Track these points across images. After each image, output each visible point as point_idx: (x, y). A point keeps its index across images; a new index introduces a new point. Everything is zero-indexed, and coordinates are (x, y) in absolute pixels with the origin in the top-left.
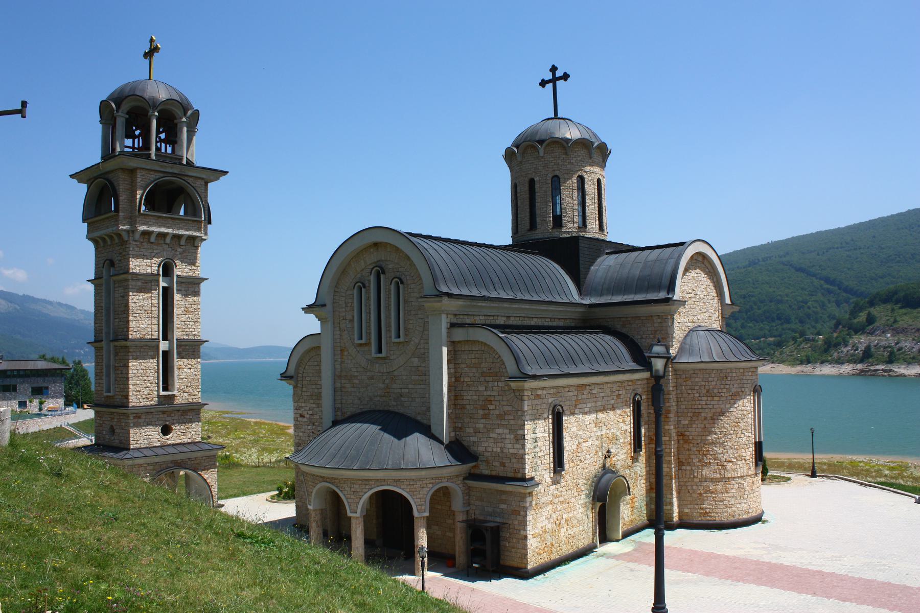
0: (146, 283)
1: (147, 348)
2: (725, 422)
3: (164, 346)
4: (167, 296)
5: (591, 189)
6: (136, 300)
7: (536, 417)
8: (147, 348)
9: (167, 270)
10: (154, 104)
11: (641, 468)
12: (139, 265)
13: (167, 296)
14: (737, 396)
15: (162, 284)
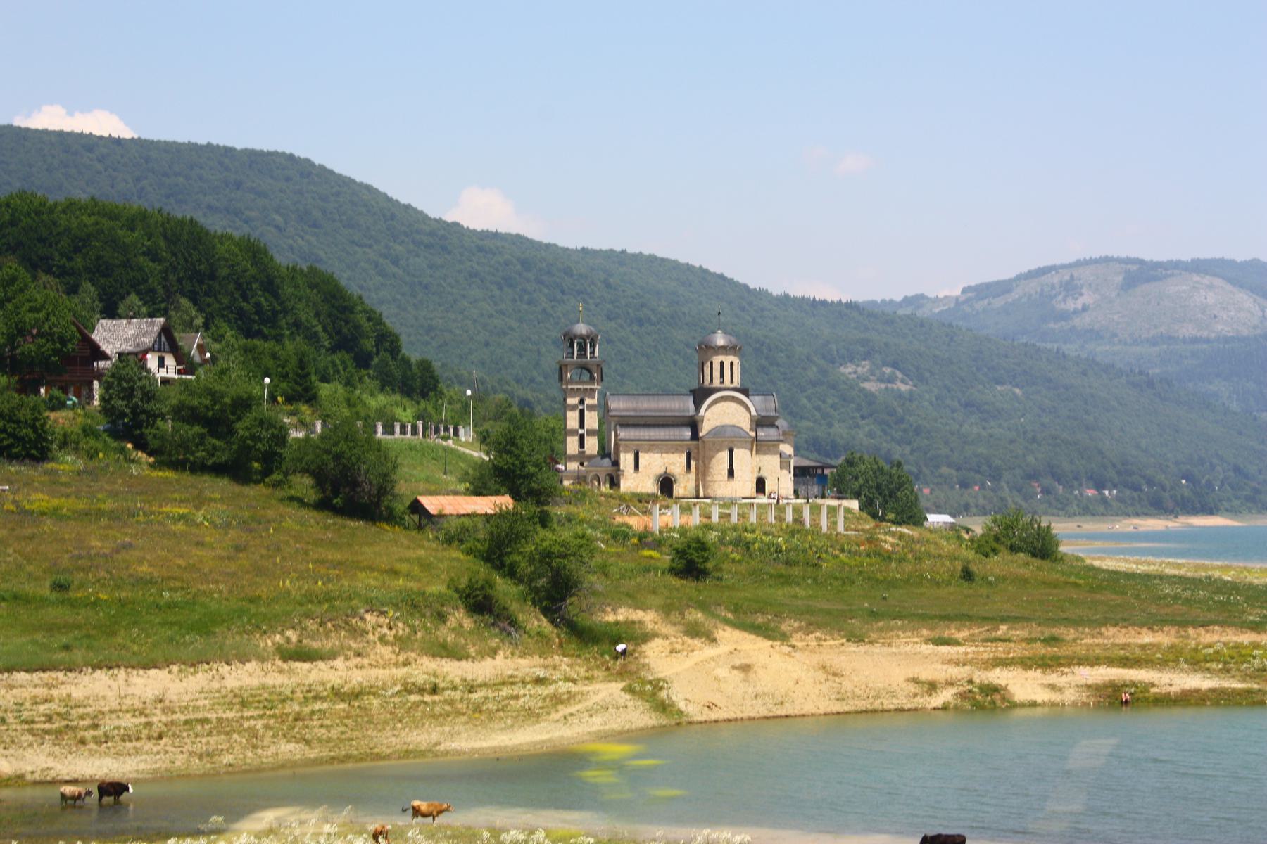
0: (574, 408)
1: (574, 432)
2: (714, 461)
3: (581, 431)
4: (582, 412)
5: (717, 367)
6: (569, 414)
7: (626, 452)
8: (574, 432)
9: (582, 402)
10: (576, 337)
11: (692, 475)
12: (570, 401)
13: (582, 412)
14: (719, 451)
15: (580, 407)
